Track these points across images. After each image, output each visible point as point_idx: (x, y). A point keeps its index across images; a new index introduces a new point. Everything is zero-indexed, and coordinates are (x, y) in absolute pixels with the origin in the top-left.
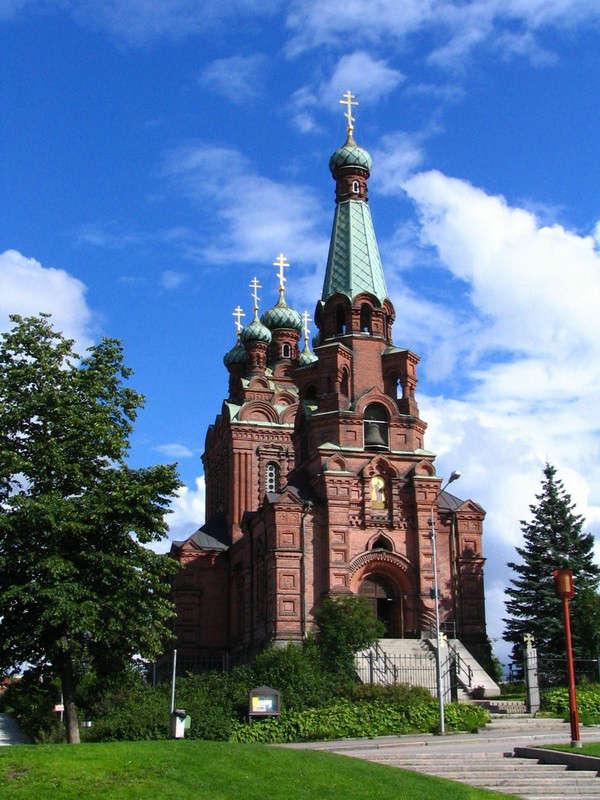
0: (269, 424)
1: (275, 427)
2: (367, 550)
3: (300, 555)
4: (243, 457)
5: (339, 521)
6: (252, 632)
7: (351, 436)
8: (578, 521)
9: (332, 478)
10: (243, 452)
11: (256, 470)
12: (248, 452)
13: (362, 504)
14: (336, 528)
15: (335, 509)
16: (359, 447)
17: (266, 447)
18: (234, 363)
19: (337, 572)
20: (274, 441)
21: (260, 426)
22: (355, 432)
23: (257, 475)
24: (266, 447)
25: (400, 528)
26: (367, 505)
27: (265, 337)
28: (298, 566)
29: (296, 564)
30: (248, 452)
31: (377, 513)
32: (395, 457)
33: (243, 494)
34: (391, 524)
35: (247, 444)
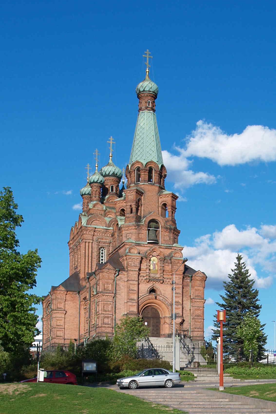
5: (133, 279)
8: (251, 283)
15: (131, 272)
32: (163, 247)
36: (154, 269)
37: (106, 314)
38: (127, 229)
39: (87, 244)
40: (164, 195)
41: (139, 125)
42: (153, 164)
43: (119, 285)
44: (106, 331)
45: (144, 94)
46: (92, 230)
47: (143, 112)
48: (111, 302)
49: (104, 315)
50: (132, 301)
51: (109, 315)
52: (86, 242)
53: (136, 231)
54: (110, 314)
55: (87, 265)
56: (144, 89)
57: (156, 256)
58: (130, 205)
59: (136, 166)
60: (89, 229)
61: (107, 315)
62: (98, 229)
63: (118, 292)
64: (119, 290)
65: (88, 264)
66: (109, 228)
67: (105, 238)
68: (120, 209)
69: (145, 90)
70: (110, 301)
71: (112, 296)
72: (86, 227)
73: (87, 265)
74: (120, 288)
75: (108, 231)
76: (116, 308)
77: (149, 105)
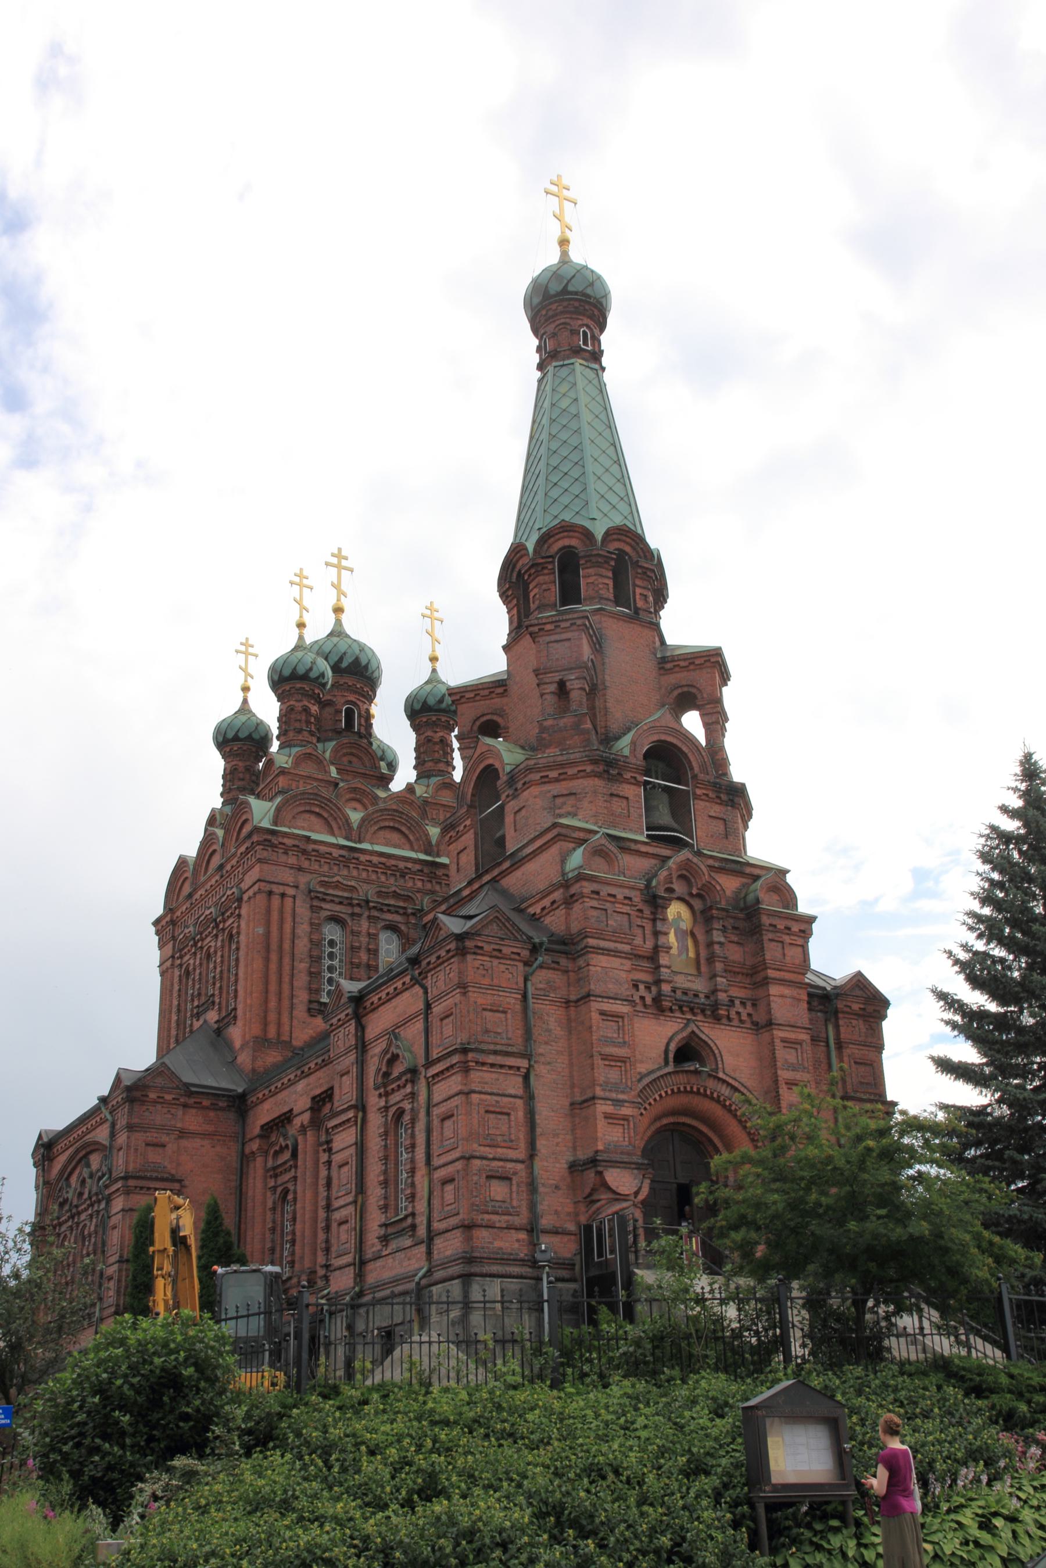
0: (331, 839)
1: (343, 847)
2: (667, 1063)
3: (523, 1063)
4: (276, 901)
5: (612, 988)
6: (361, 1264)
7: (618, 806)
9: (595, 887)
10: (275, 888)
11: (303, 929)
12: (291, 891)
13: (653, 957)
14: (606, 1006)
16: (635, 832)
17: (323, 884)
18: (236, 738)
19: (609, 1108)
20: (340, 875)
21: (316, 842)
22: (627, 798)
23: (306, 940)
24: (323, 884)
25: (729, 1019)
26: (664, 960)
27: (323, 675)
28: (520, 1092)
29: (514, 1085)
30: (291, 891)
31: (681, 982)
33: (273, 978)
34: (715, 1006)
35: (287, 876)
36: (684, 956)
37: (494, 1159)
38: (553, 774)
39: (276, 901)
40: (685, 660)
41: (553, 405)
42: (628, 540)
43: (546, 1018)
44: (497, 1244)
45: (565, 304)
46: (294, 846)
47: (566, 362)
48: (515, 1097)
49: (485, 1162)
50: (614, 1095)
51: (510, 1165)
52: (270, 893)
53: (597, 782)
54: (512, 1161)
55: (273, 987)
56: (567, 284)
57: (687, 898)
58: (557, 679)
59: (560, 544)
60: (286, 841)
61: (501, 1164)
62: (316, 847)
63: (541, 1051)
64: (546, 1043)
65: (280, 982)
66: (358, 846)
67: (345, 882)
68: (478, 723)
69: (570, 288)
70: (512, 1092)
71: (518, 1068)
72: (273, 832)
73: (273, 987)
74: (549, 1031)
75: (356, 855)
76: (539, 1131)
77: (585, 343)
